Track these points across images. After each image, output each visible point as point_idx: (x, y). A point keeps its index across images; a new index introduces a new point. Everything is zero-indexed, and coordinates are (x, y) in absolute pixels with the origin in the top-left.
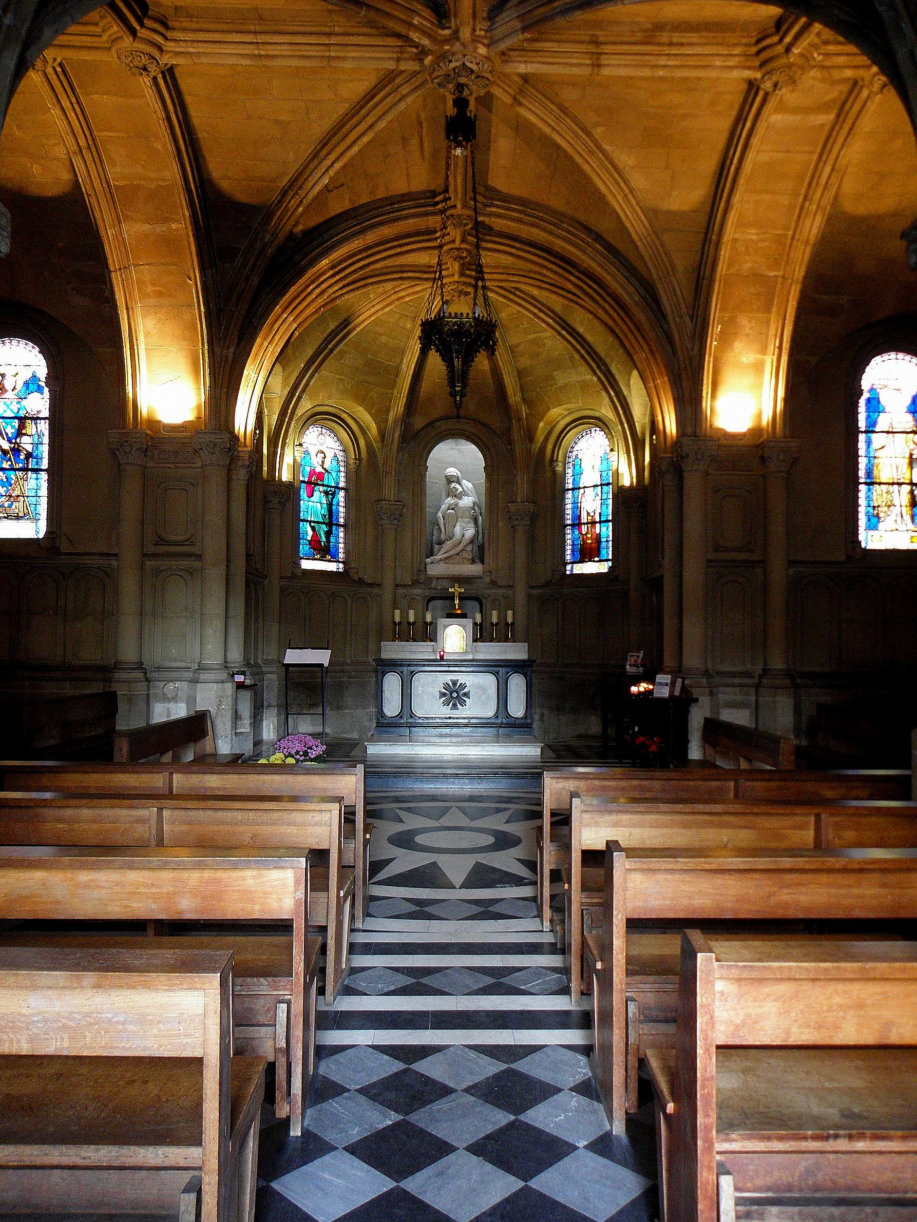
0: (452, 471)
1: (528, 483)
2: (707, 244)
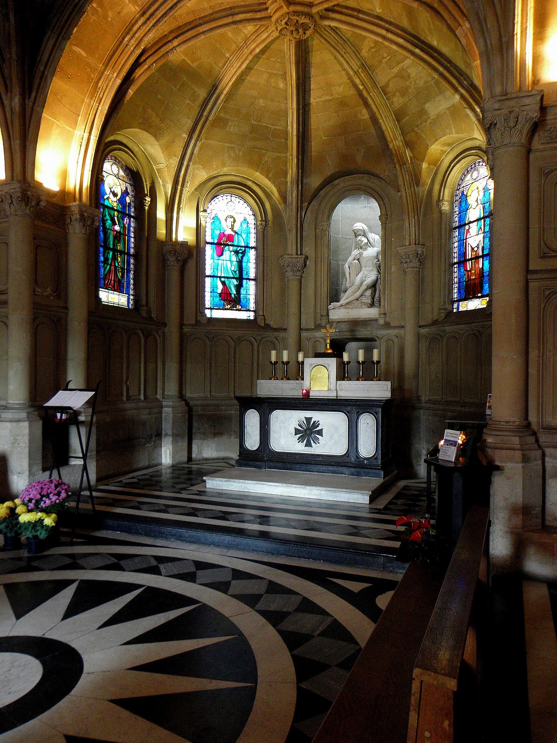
0: (359, 226)
1: (421, 224)
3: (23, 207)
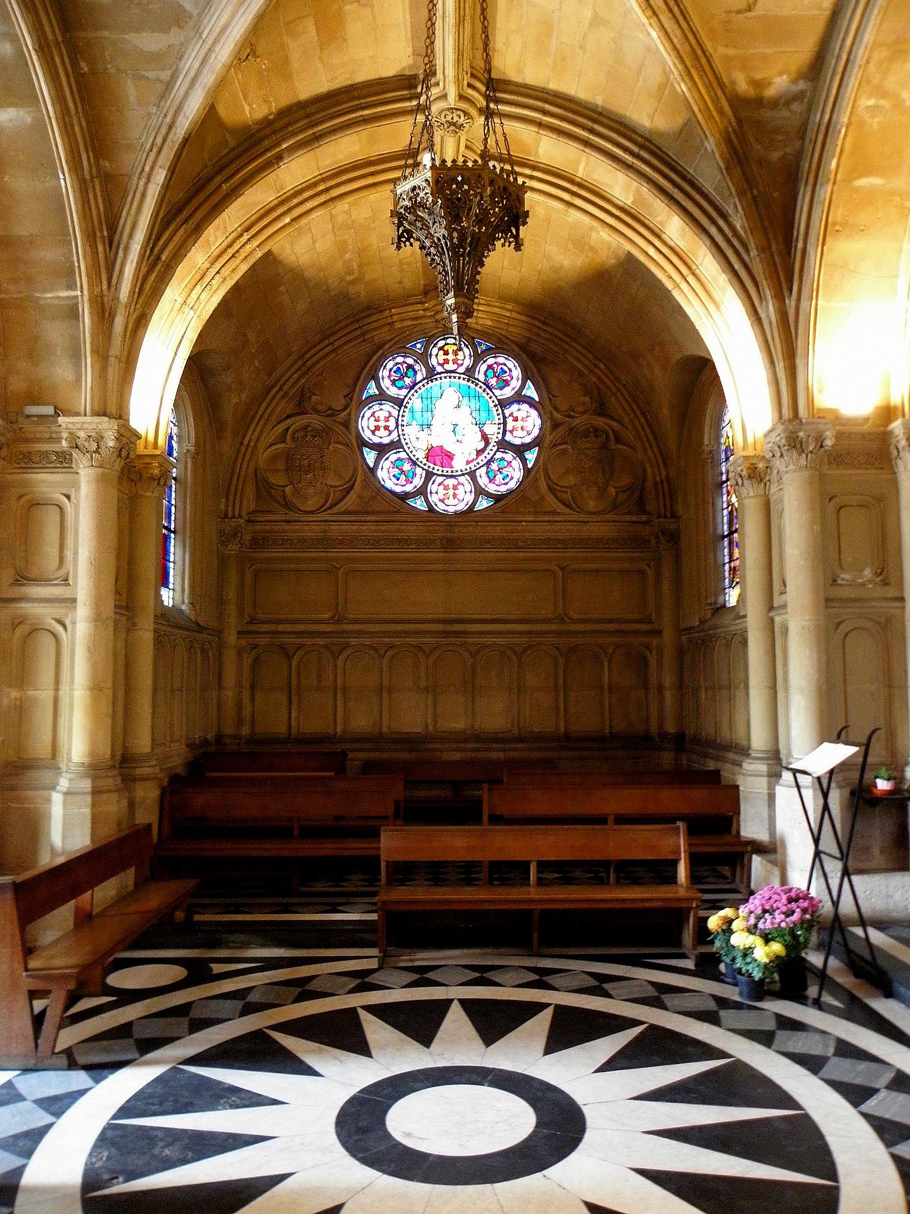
3: (795, 454)
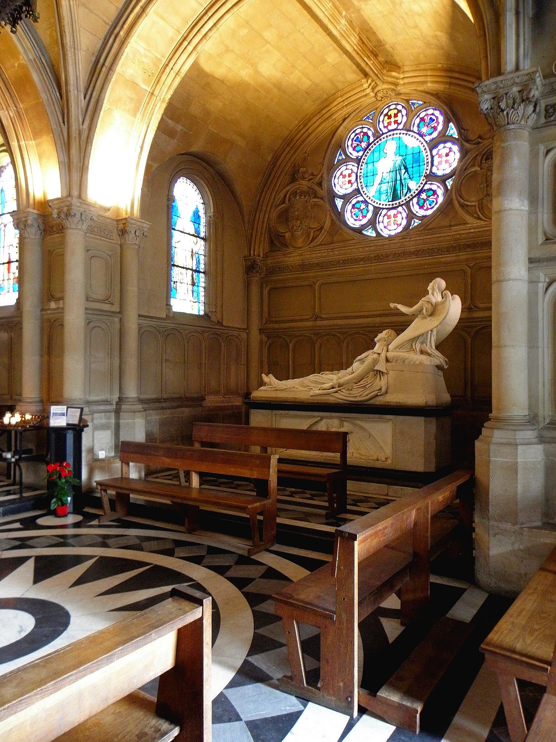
2: (113, 37)
